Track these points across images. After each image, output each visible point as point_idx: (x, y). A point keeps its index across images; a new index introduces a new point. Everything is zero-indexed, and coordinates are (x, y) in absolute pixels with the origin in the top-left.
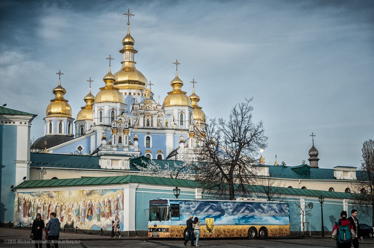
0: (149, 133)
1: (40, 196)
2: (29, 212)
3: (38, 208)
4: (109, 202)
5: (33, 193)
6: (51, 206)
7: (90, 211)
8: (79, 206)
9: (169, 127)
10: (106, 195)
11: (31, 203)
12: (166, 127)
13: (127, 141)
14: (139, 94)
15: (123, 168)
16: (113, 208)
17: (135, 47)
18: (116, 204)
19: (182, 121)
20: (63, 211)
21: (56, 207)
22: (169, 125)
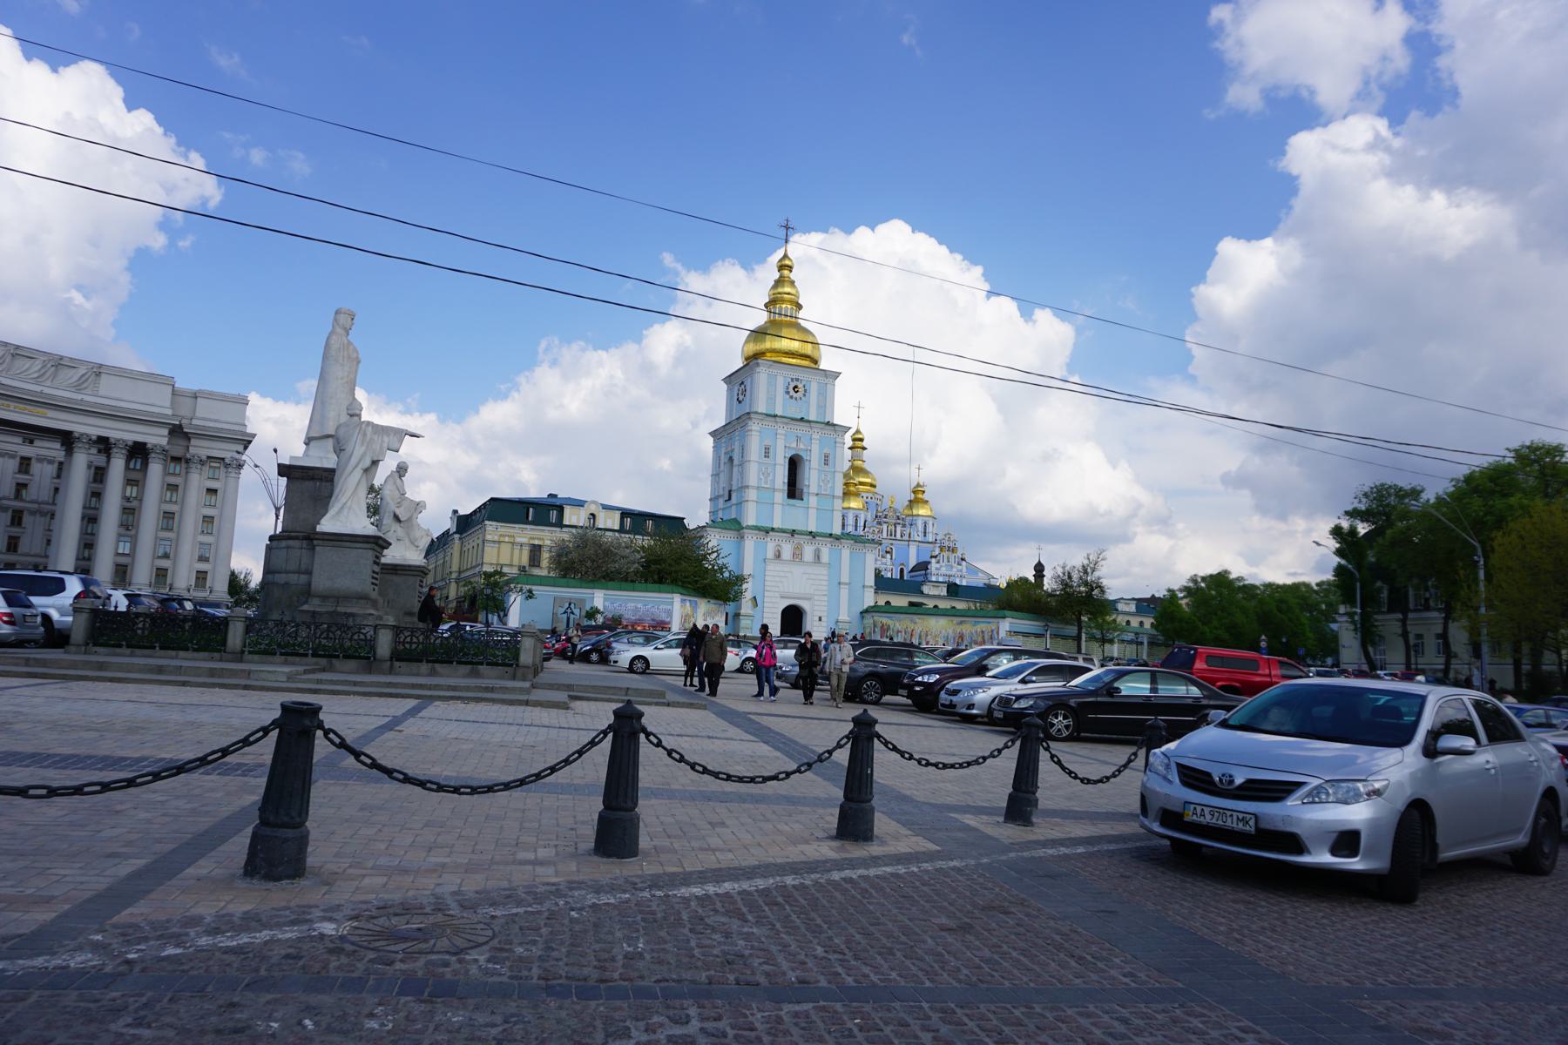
1: (900, 621)
3: (898, 632)
16: (987, 637)
17: (865, 444)
19: (925, 533)
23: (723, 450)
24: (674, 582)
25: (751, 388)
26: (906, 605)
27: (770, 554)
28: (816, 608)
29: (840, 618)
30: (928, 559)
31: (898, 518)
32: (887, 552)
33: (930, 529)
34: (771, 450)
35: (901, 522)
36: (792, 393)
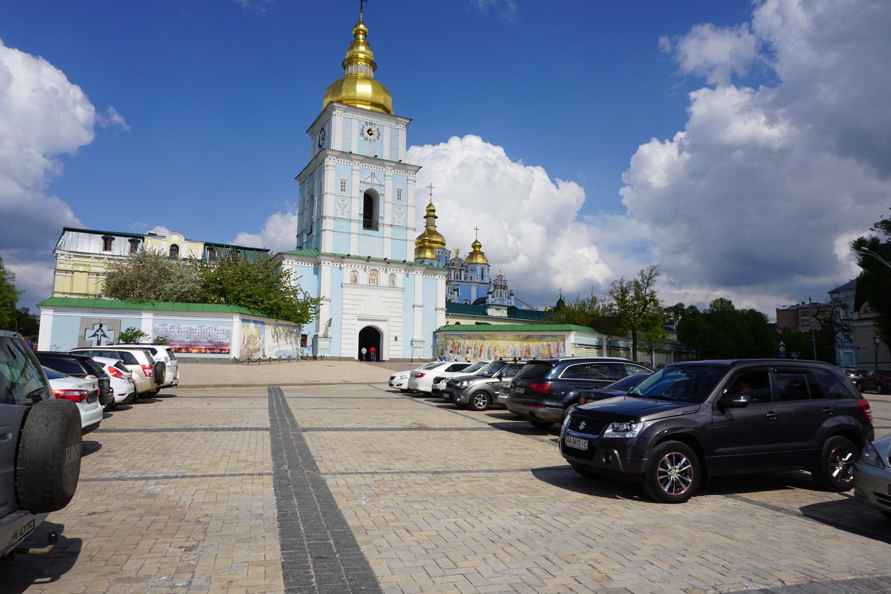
0: (458, 285)
2: (458, 348)
3: (469, 348)
4: (549, 345)
5: (462, 336)
6: (483, 347)
7: (527, 353)
8: (515, 348)
9: (473, 281)
10: (545, 339)
11: (460, 344)
12: (471, 281)
13: (450, 291)
14: (442, 253)
15: (503, 316)
17: (436, 214)
18: (556, 347)
19: (482, 276)
20: (497, 352)
21: (489, 347)
22: (473, 278)
23: (306, 190)
24: (237, 301)
25: (329, 134)
26: (474, 324)
27: (347, 279)
28: (392, 329)
29: (416, 337)
30: (485, 295)
31: (462, 265)
32: (455, 290)
33: (486, 273)
34: (347, 185)
35: (464, 268)
36: (367, 135)
